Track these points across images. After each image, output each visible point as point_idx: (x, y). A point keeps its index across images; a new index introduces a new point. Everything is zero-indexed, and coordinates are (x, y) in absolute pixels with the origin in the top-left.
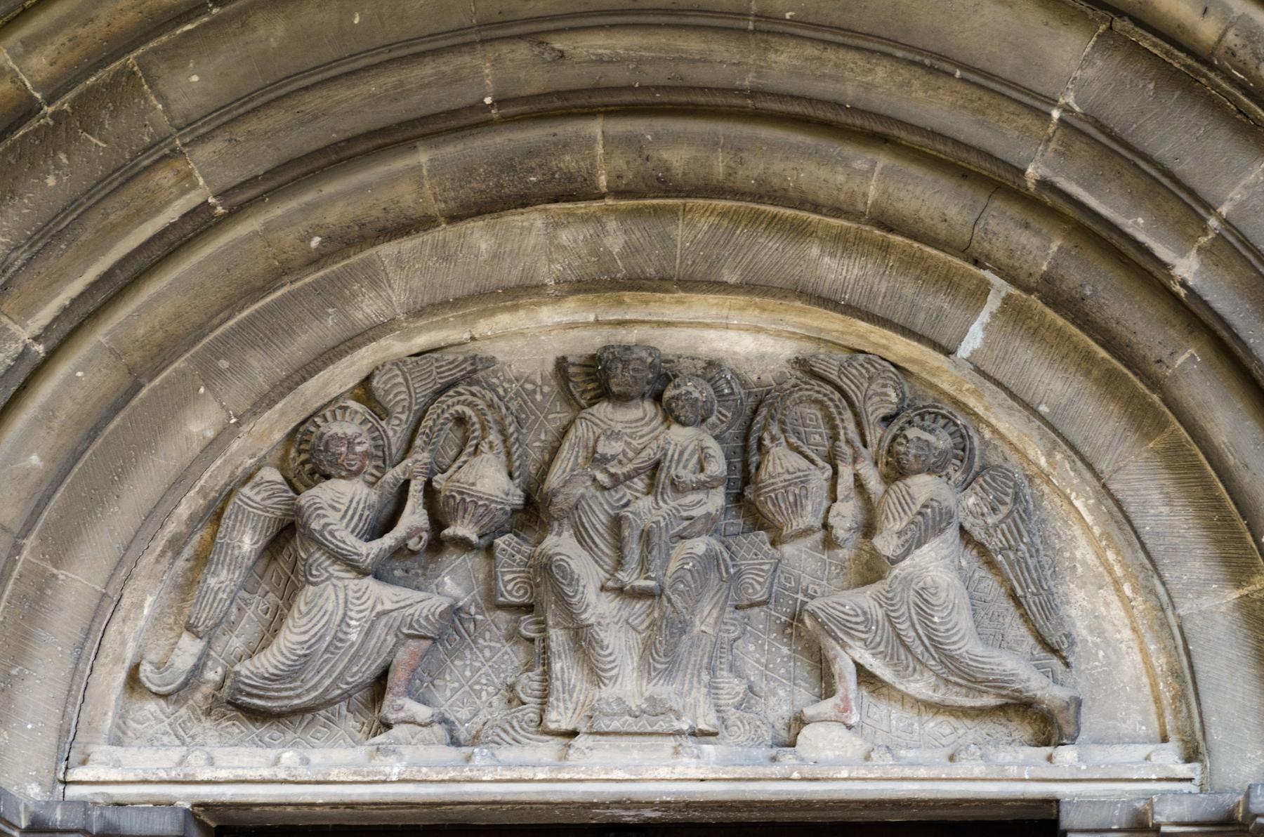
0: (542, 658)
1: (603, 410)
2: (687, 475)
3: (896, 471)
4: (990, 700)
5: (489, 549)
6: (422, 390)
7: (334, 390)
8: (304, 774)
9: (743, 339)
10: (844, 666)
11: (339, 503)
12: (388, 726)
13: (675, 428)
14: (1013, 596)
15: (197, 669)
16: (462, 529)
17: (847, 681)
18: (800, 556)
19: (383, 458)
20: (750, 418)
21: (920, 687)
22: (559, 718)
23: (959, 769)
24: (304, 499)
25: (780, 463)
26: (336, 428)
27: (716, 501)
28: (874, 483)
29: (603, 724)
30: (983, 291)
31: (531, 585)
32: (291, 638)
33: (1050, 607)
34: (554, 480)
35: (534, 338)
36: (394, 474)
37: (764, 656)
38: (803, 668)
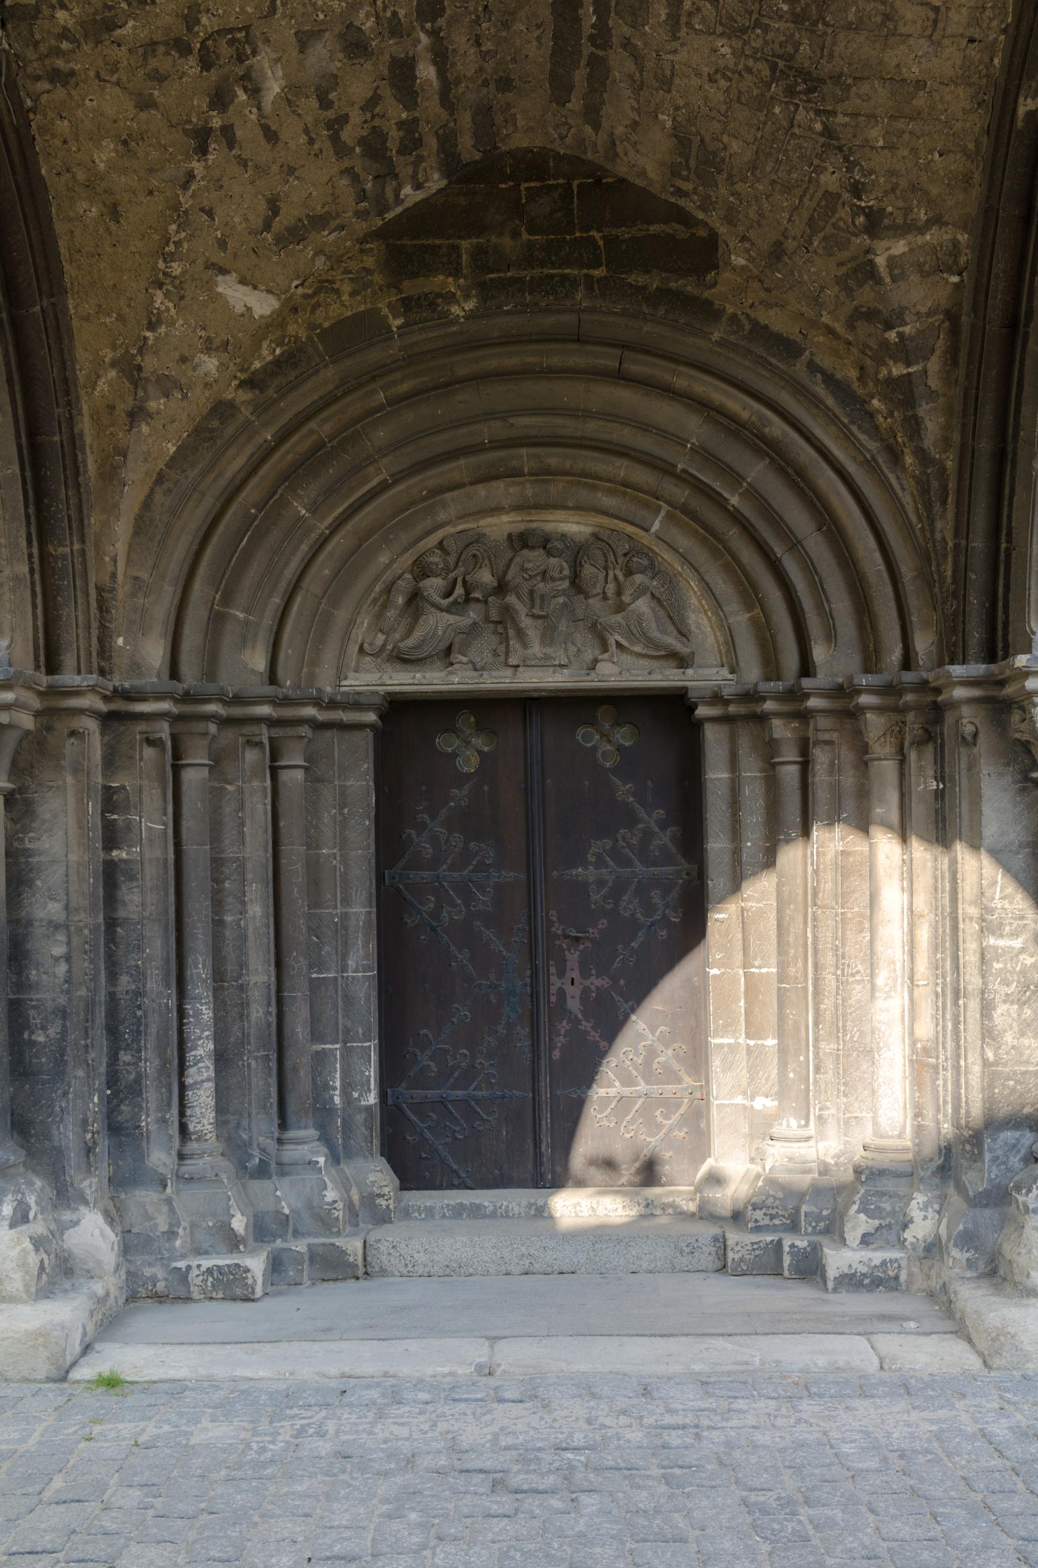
1: (525, 552)
2: (556, 575)
3: (629, 573)
4: (662, 653)
5: (486, 602)
7: (430, 546)
8: (424, 681)
9: (574, 526)
10: (611, 641)
11: (433, 586)
12: (452, 664)
14: (669, 616)
15: (384, 645)
18: (595, 603)
19: (448, 570)
20: (577, 553)
21: (638, 649)
22: (512, 661)
23: (653, 677)
24: (421, 584)
25: (588, 570)
26: (431, 559)
27: (566, 584)
28: (621, 577)
29: (528, 663)
30: (660, 508)
32: (417, 634)
33: (683, 620)
34: (509, 577)
35: (500, 526)
36: (452, 575)
37: (582, 638)
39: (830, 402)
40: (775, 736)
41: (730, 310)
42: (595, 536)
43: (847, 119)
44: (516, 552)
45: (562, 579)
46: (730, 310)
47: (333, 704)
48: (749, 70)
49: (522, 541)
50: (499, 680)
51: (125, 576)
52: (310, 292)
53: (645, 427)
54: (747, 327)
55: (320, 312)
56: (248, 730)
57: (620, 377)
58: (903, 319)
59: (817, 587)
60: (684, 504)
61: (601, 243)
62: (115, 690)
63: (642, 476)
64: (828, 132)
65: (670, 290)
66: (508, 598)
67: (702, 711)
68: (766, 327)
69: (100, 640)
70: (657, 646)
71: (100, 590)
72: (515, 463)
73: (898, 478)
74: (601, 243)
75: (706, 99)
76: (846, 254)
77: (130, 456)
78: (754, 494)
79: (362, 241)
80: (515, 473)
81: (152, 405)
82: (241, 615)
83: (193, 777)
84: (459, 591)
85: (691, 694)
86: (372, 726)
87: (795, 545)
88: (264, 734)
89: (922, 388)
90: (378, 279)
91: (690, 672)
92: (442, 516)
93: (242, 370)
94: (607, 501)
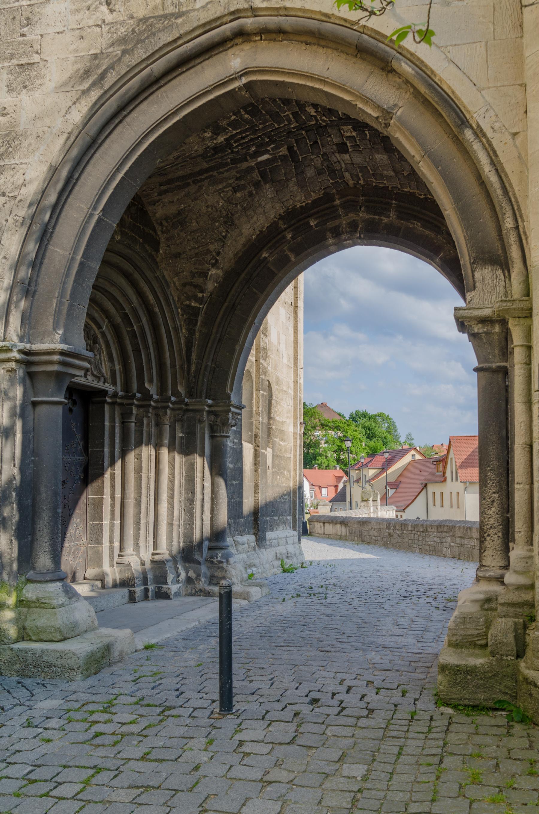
48: (220, 211)
53: (125, 295)
57: (127, 276)
64: (225, 237)
75: (200, 209)
76: (200, 267)
78: (142, 328)
87: (147, 347)
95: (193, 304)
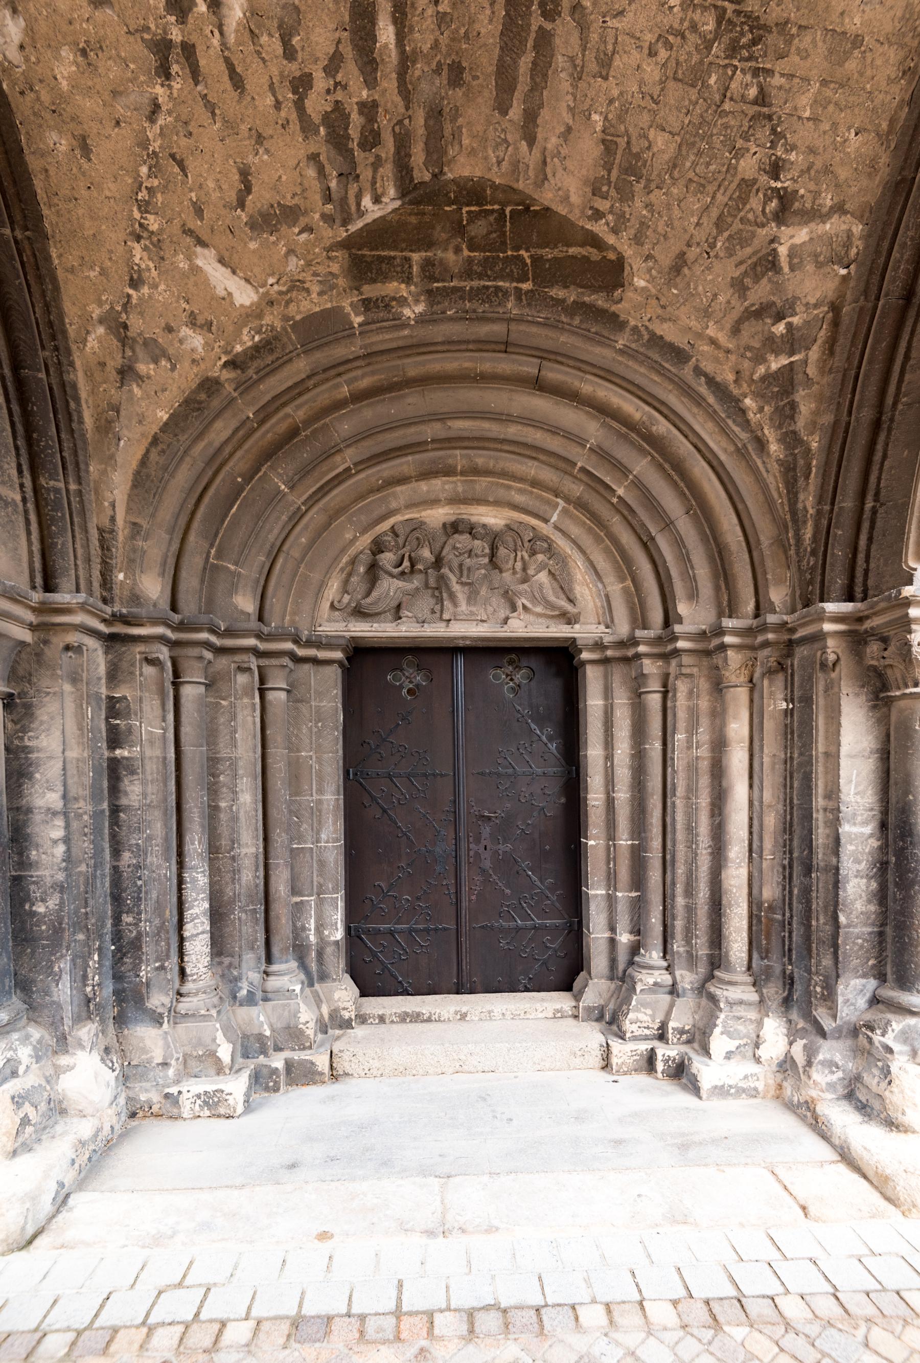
0: (440, 601)
1: (456, 536)
2: (479, 553)
3: (533, 553)
4: (557, 613)
6: (408, 530)
9: (491, 518)
11: (387, 559)
12: (400, 618)
13: (476, 542)
14: (562, 588)
15: (349, 603)
16: (420, 567)
17: (520, 609)
19: (398, 549)
20: (494, 539)
21: (539, 609)
22: (446, 616)
23: (550, 630)
25: (502, 552)
27: (486, 560)
28: (526, 556)
30: (557, 504)
31: (437, 581)
32: (375, 594)
33: (571, 590)
35: (437, 516)
38: (507, 605)
39: (711, 400)
40: (645, 672)
41: (632, 323)
42: (508, 527)
43: (783, 80)
44: (448, 536)
45: (484, 556)
46: (632, 323)
47: (309, 644)
49: (454, 527)
50: (435, 631)
51: (125, 522)
52: (284, 289)
53: (554, 430)
54: (646, 337)
55: (292, 307)
56: (238, 658)
58: (794, 310)
59: (685, 558)
60: (578, 498)
61: (528, 261)
62: (114, 615)
63: (547, 475)
65: (584, 303)
66: (442, 571)
67: (585, 655)
68: (661, 337)
69: (102, 574)
70: (553, 607)
71: (101, 531)
72: (450, 461)
73: (764, 462)
74: (528, 261)
75: (642, 83)
76: (749, 250)
77: (123, 413)
79: (329, 249)
80: (449, 472)
81: (142, 368)
82: (232, 567)
83: (189, 692)
84: (406, 563)
85: (579, 642)
86: (340, 663)
87: (668, 524)
88: (254, 663)
89: (800, 376)
90: (341, 282)
91: (577, 626)
92: (394, 505)
93: (226, 353)
94: (519, 499)
95: (774, 366)
